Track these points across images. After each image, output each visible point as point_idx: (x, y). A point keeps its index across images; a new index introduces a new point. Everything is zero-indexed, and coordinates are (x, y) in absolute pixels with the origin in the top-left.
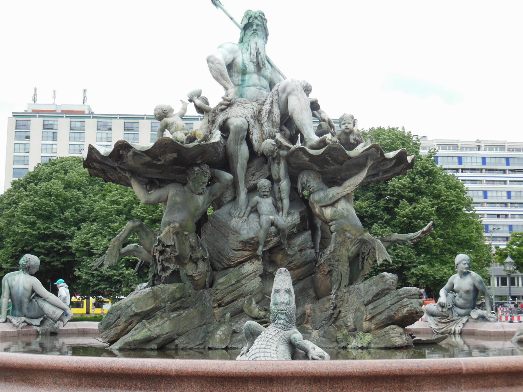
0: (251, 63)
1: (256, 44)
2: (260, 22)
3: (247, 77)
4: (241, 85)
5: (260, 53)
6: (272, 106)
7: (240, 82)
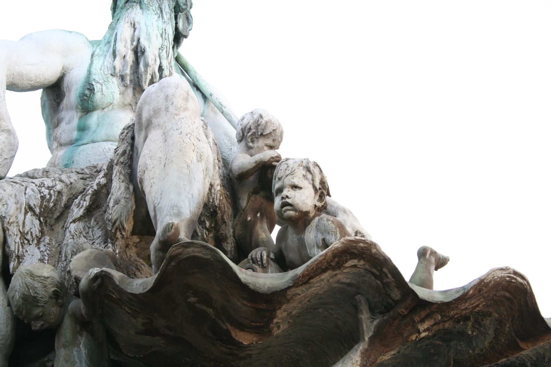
0: (115, 81)
1: (134, 26)
3: (94, 118)
4: (77, 140)
5: (143, 52)
7: (75, 134)
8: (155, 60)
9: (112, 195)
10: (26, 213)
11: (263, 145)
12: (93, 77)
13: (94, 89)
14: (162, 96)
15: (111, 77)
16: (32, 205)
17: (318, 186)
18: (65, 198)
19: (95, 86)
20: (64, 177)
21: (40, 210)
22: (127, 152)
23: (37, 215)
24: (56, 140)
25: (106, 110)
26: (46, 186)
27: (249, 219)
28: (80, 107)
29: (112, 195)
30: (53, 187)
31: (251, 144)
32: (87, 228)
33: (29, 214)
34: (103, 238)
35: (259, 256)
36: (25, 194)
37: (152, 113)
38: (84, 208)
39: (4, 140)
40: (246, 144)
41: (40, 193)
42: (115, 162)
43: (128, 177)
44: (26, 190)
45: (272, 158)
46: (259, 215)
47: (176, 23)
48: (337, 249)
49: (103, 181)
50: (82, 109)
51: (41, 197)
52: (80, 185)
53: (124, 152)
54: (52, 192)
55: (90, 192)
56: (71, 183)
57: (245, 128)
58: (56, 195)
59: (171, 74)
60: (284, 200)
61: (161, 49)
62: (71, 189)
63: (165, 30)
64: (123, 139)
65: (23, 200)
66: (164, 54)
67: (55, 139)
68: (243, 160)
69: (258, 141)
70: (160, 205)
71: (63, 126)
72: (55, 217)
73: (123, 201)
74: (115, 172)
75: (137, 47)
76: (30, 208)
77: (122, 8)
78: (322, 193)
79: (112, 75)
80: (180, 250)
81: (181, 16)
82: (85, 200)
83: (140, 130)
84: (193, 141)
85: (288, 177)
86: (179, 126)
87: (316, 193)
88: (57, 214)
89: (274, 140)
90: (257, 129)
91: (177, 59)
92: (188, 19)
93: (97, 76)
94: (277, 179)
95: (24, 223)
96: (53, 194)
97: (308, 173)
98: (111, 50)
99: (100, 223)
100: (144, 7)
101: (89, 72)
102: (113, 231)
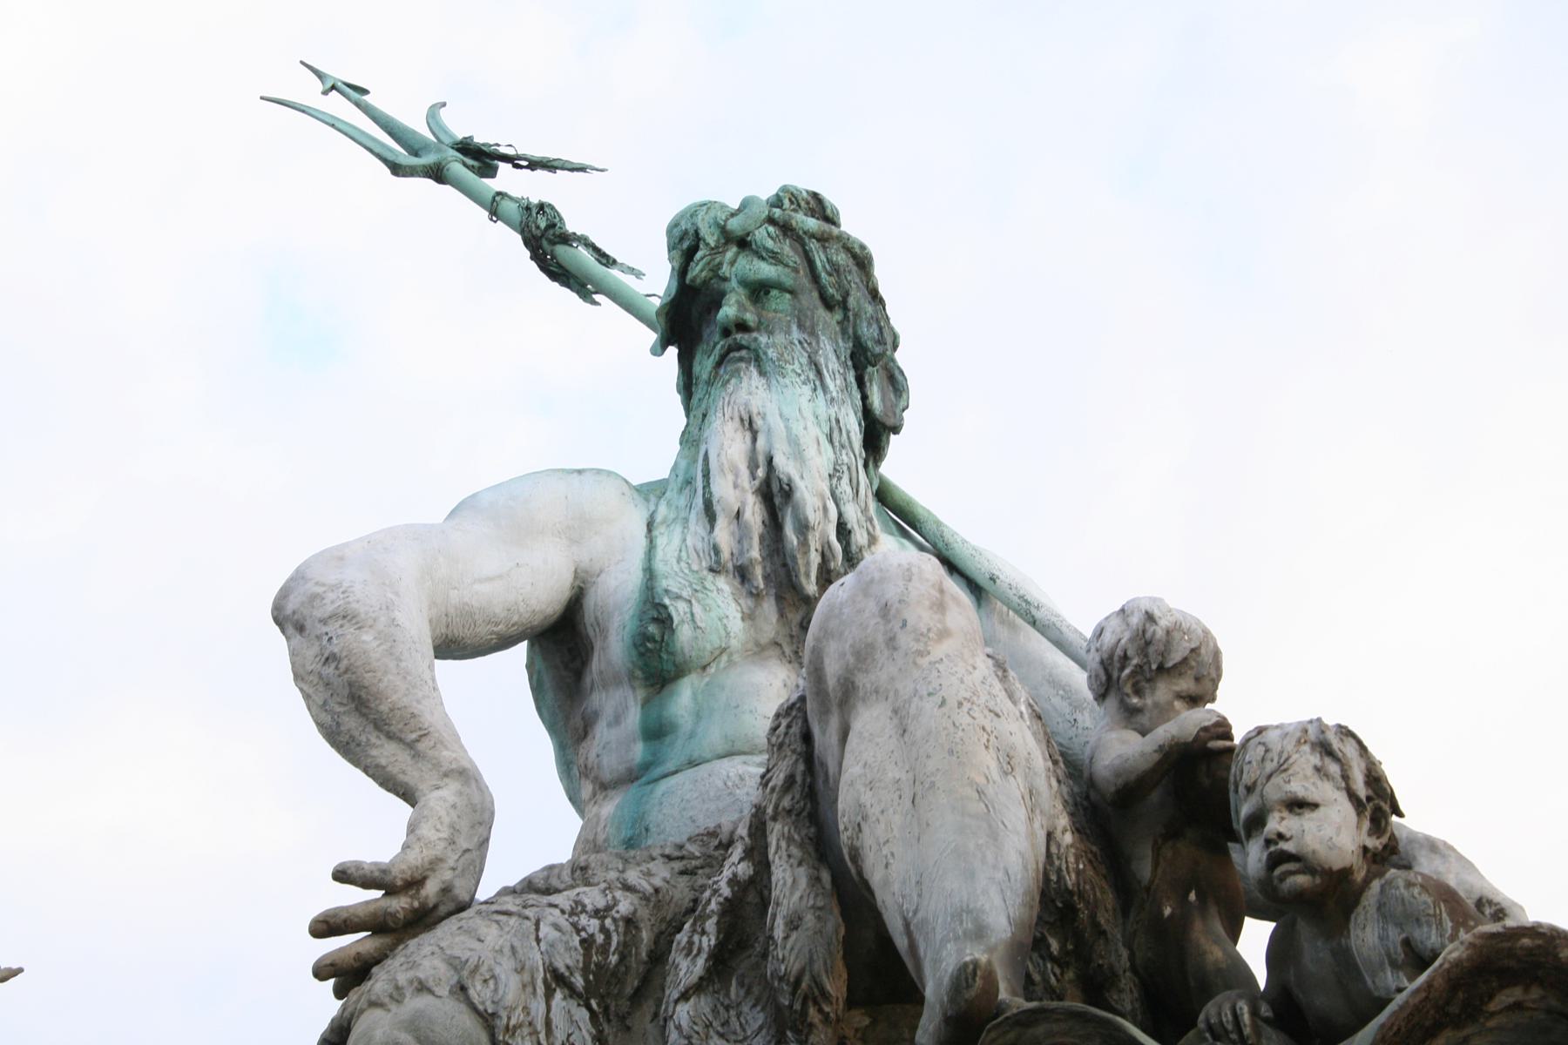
0: (724, 586)
1: (750, 426)
2: (775, 258)
3: (683, 698)
4: (646, 767)
5: (788, 492)
6: (757, 853)
7: (638, 751)
8: (825, 509)
9: (778, 904)
10: (549, 995)
11: (1170, 696)
12: (664, 583)
13: (670, 618)
14: (872, 607)
15: (710, 576)
16: (563, 969)
17: (1362, 792)
18: (646, 935)
19: (672, 610)
20: (633, 876)
21: (586, 980)
22: (799, 779)
23: (579, 996)
24: (587, 776)
25: (712, 670)
26: (589, 908)
27: (1167, 911)
28: (638, 673)
29: (778, 904)
30: (608, 908)
31: (1135, 700)
32: (722, 1010)
33: (558, 995)
34: (772, 1032)
35: (1227, 1017)
36: (538, 940)
37: (852, 660)
38: (704, 956)
39: (452, 799)
40: (1122, 702)
41: (578, 931)
42: (770, 811)
43: (811, 849)
44: (537, 929)
45: (1205, 729)
46: (1192, 896)
47: (864, 398)
48: (1457, 964)
49: (744, 870)
50: (646, 679)
51: (583, 941)
52: (681, 892)
53: (790, 781)
54: (608, 922)
55: (713, 906)
56: (657, 891)
57: (1111, 657)
58: (621, 930)
59: (873, 540)
60: (1272, 849)
61: (834, 475)
62: (658, 906)
63: (838, 421)
64: (781, 746)
65: (536, 958)
66: (845, 487)
67: (586, 772)
68: (1120, 749)
69: (1153, 690)
70: (920, 915)
71: (602, 733)
72: (629, 990)
73: (809, 919)
74: (773, 840)
75: (767, 482)
76: (556, 979)
77: (709, 383)
78: (1378, 809)
79: (711, 570)
80: (1011, 1036)
81: (875, 376)
82: (703, 933)
83: (825, 712)
84: (981, 720)
85: (1274, 780)
86: (935, 684)
87: (1360, 813)
88: (632, 983)
89: (1197, 679)
90: (1146, 655)
91: (883, 495)
92: (895, 383)
93: (672, 579)
94: (1241, 789)
95: (548, 1023)
96: (612, 928)
97: (1327, 760)
98: (699, 501)
99: (756, 990)
100: (768, 367)
101: (650, 573)
102: (797, 1006)
